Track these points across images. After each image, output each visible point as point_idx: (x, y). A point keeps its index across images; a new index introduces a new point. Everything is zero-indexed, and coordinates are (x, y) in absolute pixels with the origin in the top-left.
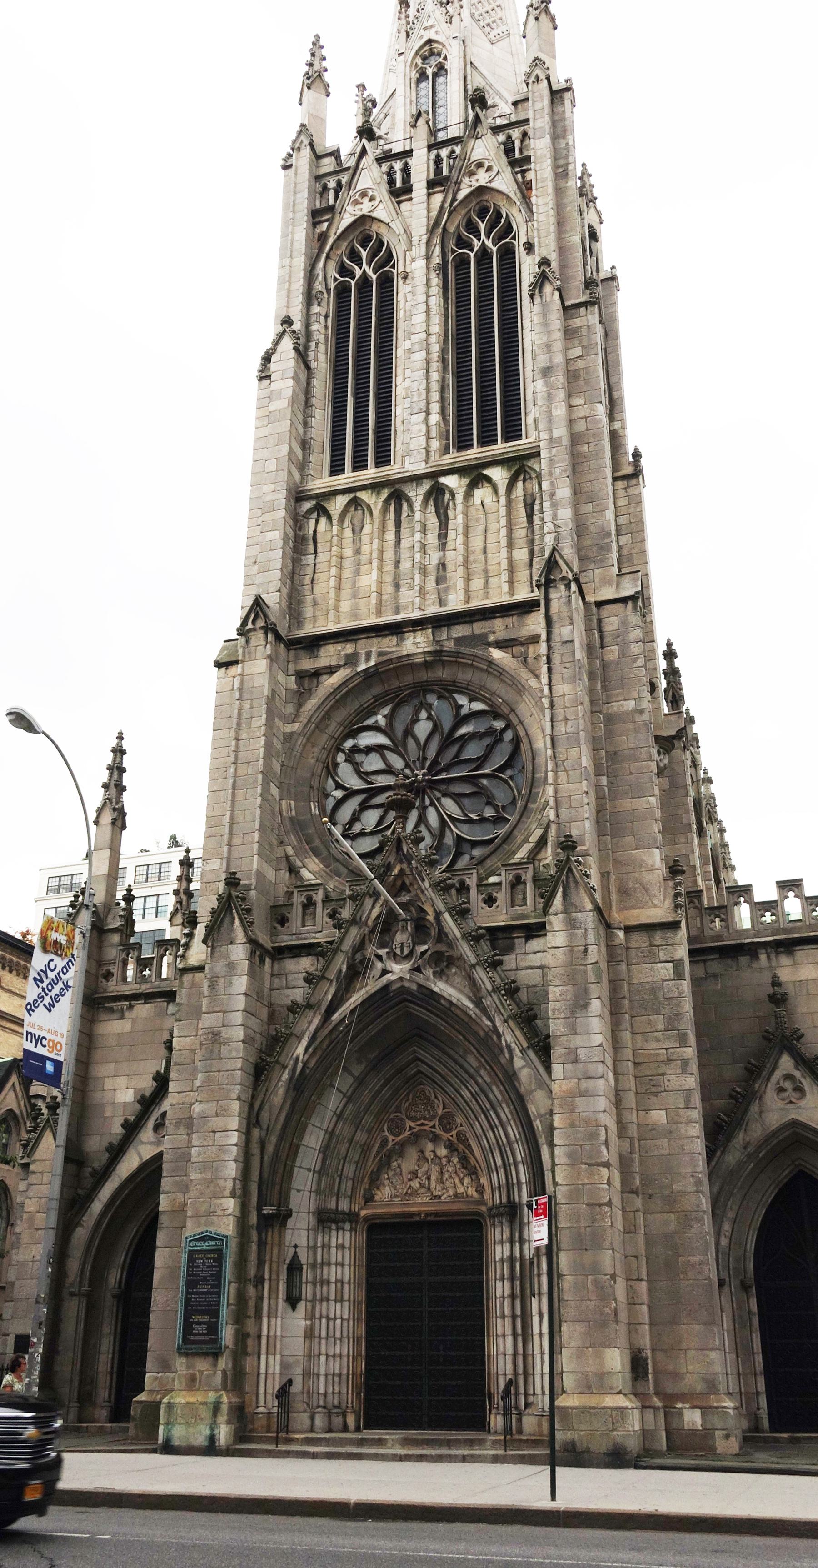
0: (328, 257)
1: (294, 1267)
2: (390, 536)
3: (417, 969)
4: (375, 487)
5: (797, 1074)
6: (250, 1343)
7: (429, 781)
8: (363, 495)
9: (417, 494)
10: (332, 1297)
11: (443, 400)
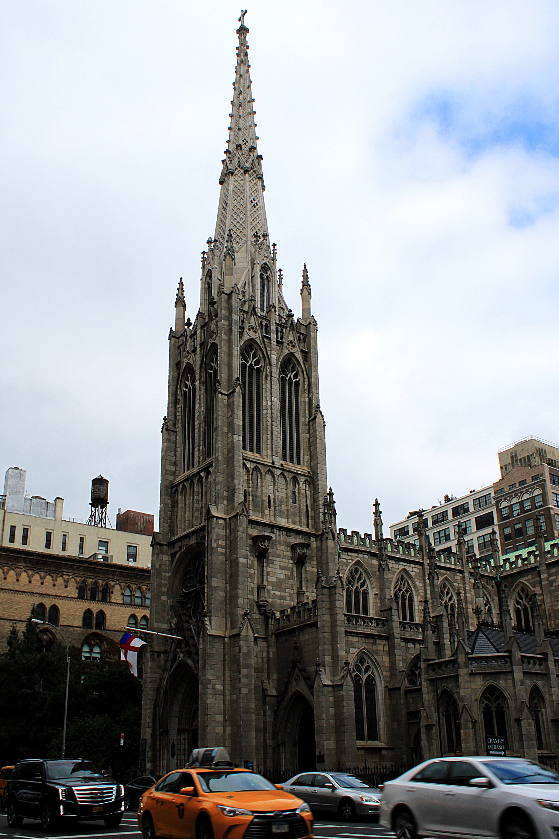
2: (192, 498)
8: (185, 483)
9: (195, 481)
11: (204, 438)
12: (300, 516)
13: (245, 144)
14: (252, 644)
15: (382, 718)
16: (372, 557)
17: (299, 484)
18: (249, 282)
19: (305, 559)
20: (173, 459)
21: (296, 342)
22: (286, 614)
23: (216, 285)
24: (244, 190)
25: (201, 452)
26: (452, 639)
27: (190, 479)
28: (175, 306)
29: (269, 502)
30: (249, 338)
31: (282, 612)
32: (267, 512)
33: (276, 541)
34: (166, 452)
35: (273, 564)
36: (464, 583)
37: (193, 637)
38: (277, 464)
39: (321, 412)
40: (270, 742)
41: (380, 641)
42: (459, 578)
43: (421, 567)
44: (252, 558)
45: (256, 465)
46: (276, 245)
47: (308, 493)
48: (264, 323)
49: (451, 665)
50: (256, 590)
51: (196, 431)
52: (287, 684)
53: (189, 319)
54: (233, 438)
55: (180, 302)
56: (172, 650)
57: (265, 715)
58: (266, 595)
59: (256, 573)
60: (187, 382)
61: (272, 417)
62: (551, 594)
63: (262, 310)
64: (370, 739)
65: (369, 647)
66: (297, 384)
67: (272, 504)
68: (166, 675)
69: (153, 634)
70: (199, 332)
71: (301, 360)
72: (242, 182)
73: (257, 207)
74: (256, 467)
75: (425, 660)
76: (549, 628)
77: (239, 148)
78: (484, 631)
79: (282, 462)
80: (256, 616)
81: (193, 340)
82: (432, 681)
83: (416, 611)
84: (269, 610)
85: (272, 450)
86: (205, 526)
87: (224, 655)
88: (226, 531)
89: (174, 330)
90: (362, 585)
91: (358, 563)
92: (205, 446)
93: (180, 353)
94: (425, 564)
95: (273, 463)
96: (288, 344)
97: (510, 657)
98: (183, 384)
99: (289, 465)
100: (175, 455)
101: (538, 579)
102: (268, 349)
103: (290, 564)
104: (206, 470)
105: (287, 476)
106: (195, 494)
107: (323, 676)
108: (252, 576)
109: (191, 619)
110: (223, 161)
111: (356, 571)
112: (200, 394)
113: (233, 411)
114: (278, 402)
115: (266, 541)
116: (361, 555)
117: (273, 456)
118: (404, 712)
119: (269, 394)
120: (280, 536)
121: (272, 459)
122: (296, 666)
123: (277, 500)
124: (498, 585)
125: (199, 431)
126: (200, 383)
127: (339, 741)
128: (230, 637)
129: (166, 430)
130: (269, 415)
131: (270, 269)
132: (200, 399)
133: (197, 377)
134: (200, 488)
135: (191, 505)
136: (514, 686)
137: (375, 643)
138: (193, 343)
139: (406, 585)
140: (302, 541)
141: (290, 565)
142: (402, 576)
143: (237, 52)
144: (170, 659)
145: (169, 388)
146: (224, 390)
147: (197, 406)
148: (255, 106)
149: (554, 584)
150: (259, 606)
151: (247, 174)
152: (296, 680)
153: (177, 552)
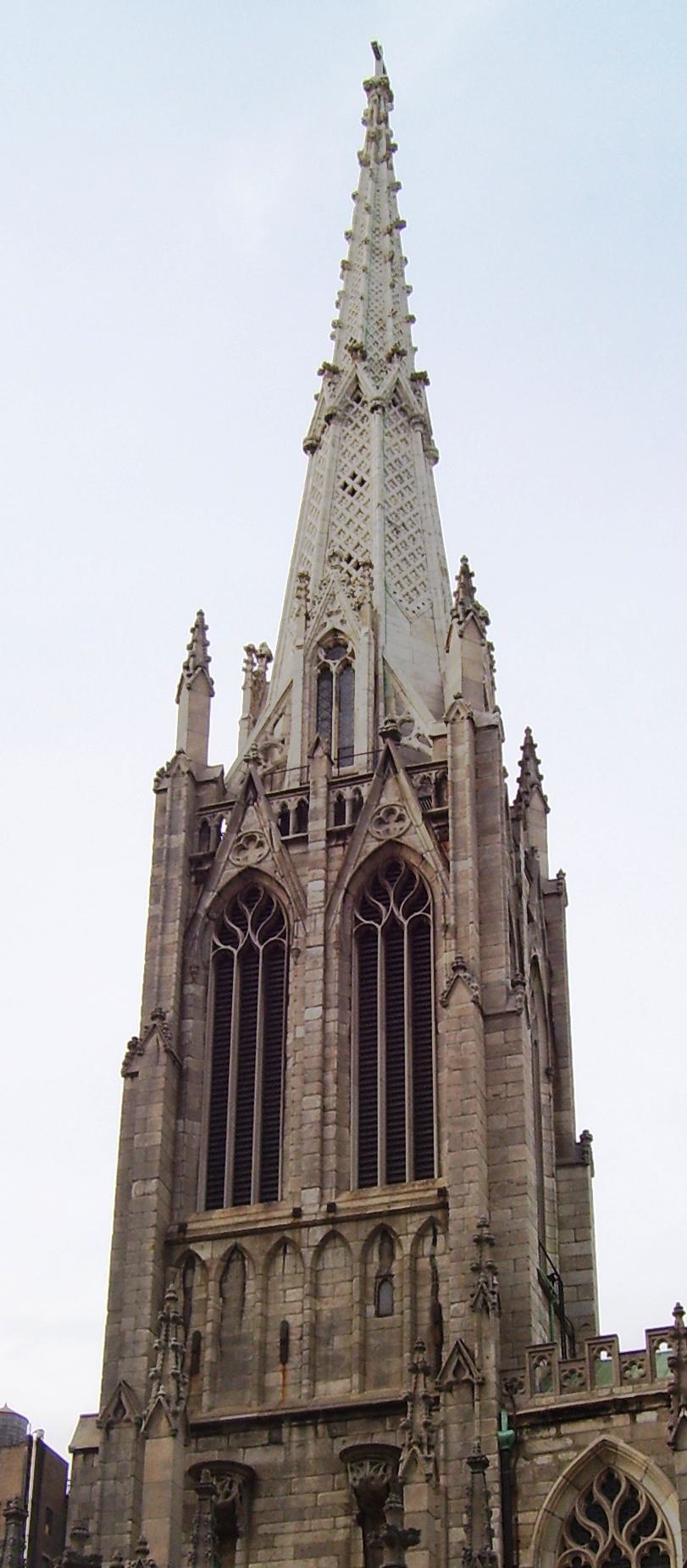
29: (285, 1342)
33: (286, 1467)
45: (230, 1243)
74: (236, 1249)
95: (297, 1213)
111: (610, 1484)
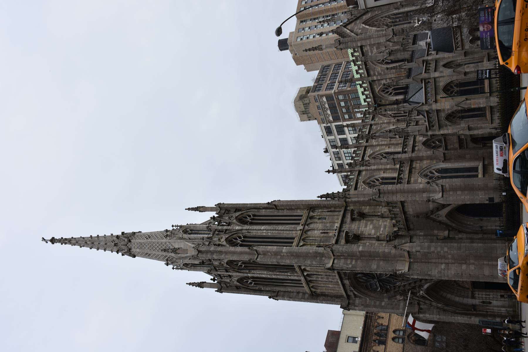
0: (248, 286)
1: (483, 302)
2: (320, 282)
3: (422, 290)
4: (308, 285)
5: (434, 215)
6: (499, 314)
7: (377, 279)
8: (311, 285)
9: (309, 279)
10: (489, 297)
11: (283, 272)
12: (334, 215)
13: (114, 241)
14: (415, 244)
15: (463, 164)
16: (361, 174)
17: (314, 216)
18: (192, 241)
19: (360, 212)
20: (295, 294)
21: (230, 215)
22: (395, 223)
23: (192, 261)
24: (140, 243)
25: (292, 274)
26: (413, 120)
27: (308, 282)
28: (203, 288)
29: (324, 233)
30: (225, 242)
31: (394, 226)
32: (331, 234)
34: (290, 298)
35: (363, 232)
36: (378, 124)
37: (410, 284)
38: (301, 227)
39: (272, 202)
40: (480, 236)
41: (413, 165)
42: (375, 127)
43: (367, 148)
44: (359, 244)
45: (301, 240)
46: (173, 225)
47: (320, 210)
48: (217, 233)
49: (430, 115)
50: (379, 242)
51: (279, 277)
52: (440, 222)
53: (211, 279)
54: (284, 252)
55: (201, 285)
56: (418, 299)
57: (461, 239)
58: (383, 236)
59: (369, 241)
60: (249, 282)
61: (273, 230)
62: (386, 74)
63: (209, 234)
64: (477, 171)
65: (417, 171)
66: (254, 215)
67: (326, 231)
68: (434, 304)
69: (407, 312)
70: (219, 273)
71: (240, 213)
72: (135, 244)
73: (150, 236)
74: (303, 240)
75: (427, 131)
76: (405, 75)
77: (116, 245)
78: (408, 98)
79: (301, 225)
80: (396, 242)
81: (223, 277)
82: (440, 127)
83: (395, 150)
84: (393, 233)
85: (293, 230)
86: (337, 272)
87: (422, 262)
88: (342, 259)
89: (217, 289)
90: (378, 180)
91: (364, 182)
92: (288, 272)
93: (231, 286)
94: (365, 145)
95: (301, 230)
96: (230, 220)
97: (425, 80)
98: (250, 285)
99: (303, 221)
100: (293, 292)
101: (377, 82)
102: (232, 231)
103: (363, 222)
104: (303, 271)
105: (309, 222)
106: (317, 279)
107: (436, 198)
108: (372, 244)
109: (397, 285)
110: (123, 255)
111: (370, 184)
112: (257, 273)
113: (268, 252)
114: (264, 226)
115: (349, 234)
116: (359, 181)
117: (296, 230)
118: (459, 151)
119: (259, 232)
120: (346, 227)
121: (298, 230)
122: (429, 216)
123: (324, 228)
124: (379, 105)
125: (279, 275)
126: (249, 273)
127: (479, 189)
128: (410, 258)
129: (277, 297)
130: (272, 232)
131: (186, 229)
132: (259, 274)
133: (246, 275)
134: (314, 276)
135: (324, 282)
136: (443, 77)
137: (415, 168)
138: (226, 277)
139: (379, 156)
140: (349, 214)
141: (365, 221)
142: (373, 158)
143: (64, 244)
144: (424, 301)
145: (251, 294)
146: (255, 257)
147: (264, 276)
148: (94, 235)
149: (380, 72)
150: (390, 240)
151: (132, 241)
152: (438, 217)
153: (354, 294)
